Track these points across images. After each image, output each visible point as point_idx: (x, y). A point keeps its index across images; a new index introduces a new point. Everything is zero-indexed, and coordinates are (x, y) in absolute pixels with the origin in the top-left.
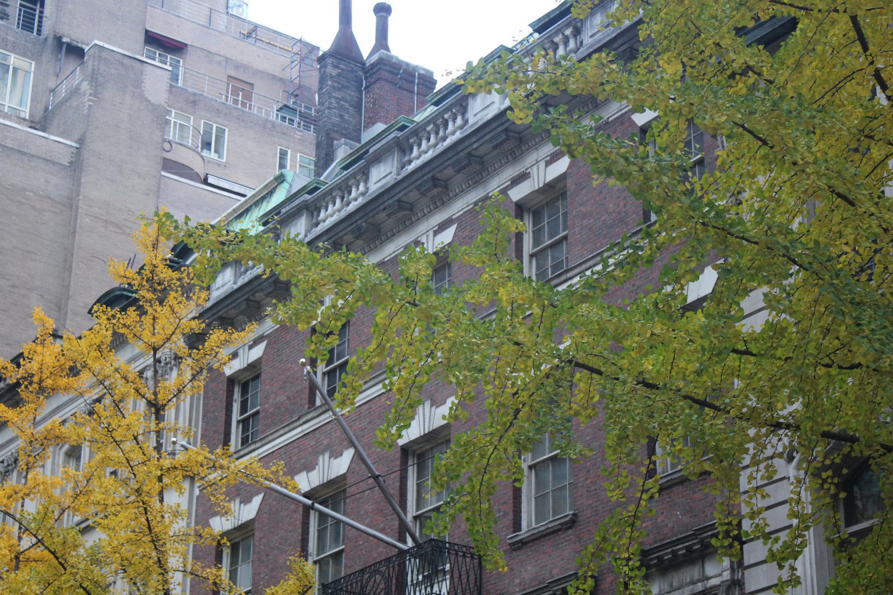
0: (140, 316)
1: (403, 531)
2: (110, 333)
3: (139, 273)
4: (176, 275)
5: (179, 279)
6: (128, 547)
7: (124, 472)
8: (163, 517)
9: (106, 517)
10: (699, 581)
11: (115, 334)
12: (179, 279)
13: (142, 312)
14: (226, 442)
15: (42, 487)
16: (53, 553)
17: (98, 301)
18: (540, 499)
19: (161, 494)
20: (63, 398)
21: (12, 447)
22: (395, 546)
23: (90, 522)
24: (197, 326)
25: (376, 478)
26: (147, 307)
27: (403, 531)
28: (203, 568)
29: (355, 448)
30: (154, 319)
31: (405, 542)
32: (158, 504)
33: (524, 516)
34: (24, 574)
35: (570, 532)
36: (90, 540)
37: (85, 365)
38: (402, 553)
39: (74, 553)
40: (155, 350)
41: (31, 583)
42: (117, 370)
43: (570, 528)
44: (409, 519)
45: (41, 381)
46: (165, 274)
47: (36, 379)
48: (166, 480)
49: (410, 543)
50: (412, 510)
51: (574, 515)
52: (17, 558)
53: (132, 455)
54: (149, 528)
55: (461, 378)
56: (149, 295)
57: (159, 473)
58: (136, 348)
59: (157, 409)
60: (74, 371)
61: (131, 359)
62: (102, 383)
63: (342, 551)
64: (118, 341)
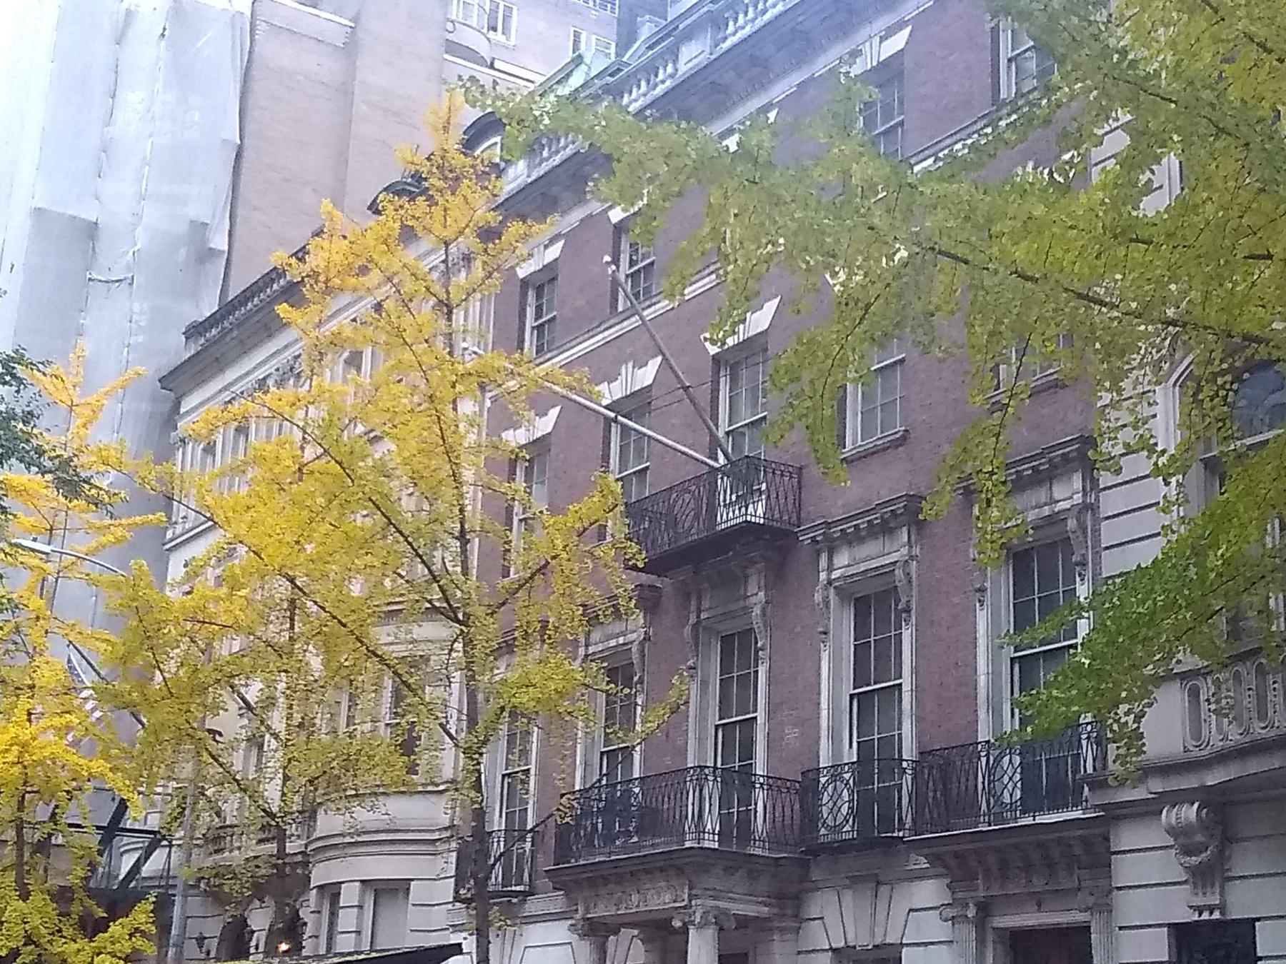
0: (430, 206)
1: (714, 446)
2: (397, 225)
3: (428, 159)
4: (469, 161)
5: (472, 166)
6: (419, 458)
7: (416, 377)
8: (457, 426)
9: (395, 426)
10: (1046, 504)
11: (403, 227)
12: (472, 166)
13: (431, 201)
14: (521, 347)
15: (327, 395)
16: (340, 463)
17: (385, 189)
18: (867, 415)
19: (454, 402)
20: (345, 299)
21: (294, 350)
22: (706, 464)
23: (378, 433)
24: (494, 219)
25: (686, 389)
26: (437, 197)
27: (714, 446)
28: (501, 483)
29: (664, 355)
30: (445, 210)
31: (716, 460)
32: (451, 414)
33: (848, 432)
34: (308, 485)
35: (900, 449)
36: (379, 451)
37: (371, 260)
38: (714, 470)
39: (361, 464)
40: (447, 244)
41: (317, 493)
42: (404, 266)
43: (901, 445)
44: (721, 434)
45: (327, 280)
46: (458, 160)
47: (322, 278)
48: (459, 388)
49: (722, 460)
50: (724, 427)
51: (906, 431)
52: (300, 469)
53: (425, 359)
54: (443, 438)
55: (812, 263)
56: (441, 184)
57: (454, 378)
58: (425, 244)
59: (446, 308)
60: (364, 270)
61: (424, 257)
62: (389, 279)
63: (647, 468)
64: (408, 235)
